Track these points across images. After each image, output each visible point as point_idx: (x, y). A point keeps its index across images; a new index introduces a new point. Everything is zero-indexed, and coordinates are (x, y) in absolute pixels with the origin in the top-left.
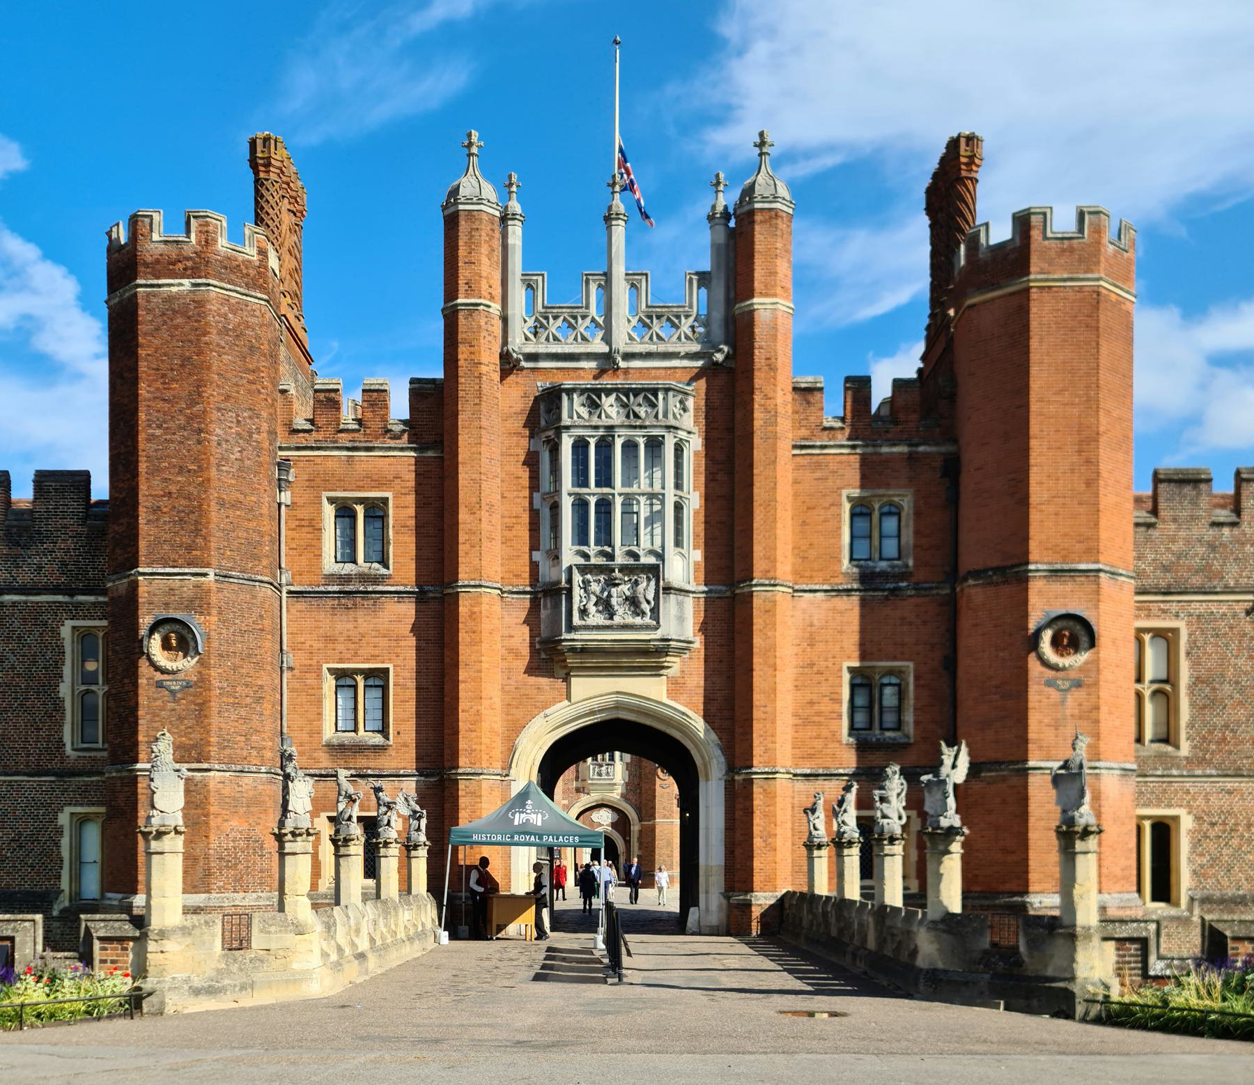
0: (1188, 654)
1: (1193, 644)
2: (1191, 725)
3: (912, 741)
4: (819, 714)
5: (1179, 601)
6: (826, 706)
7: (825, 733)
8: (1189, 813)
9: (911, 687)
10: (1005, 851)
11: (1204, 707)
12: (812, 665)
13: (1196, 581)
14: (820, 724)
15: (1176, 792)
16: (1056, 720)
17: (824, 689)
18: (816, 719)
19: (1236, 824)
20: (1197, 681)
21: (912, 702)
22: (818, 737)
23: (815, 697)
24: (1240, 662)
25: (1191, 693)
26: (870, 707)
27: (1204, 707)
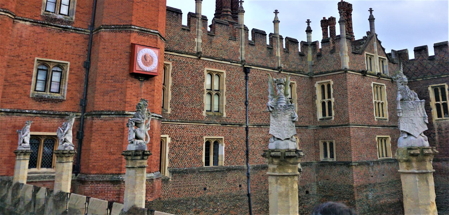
0: (172, 74)
1: (174, 70)
2: (171, 102)
3: (65, 99)
4: (19, 81)
5: (170, 54)
6: (23, 78)
7: (21, 91)
8: (169, 137)
9: (68, 73)
10: (110, 153)
11: (176, 95)
12: (18, 56)
13: (176, 48)
14: (18, 86)
15: (165, 128)
16: (138, 94)
17: (24, 69)
18: (17, 83)
19: (185, 141)
20: (174, 85)
21: (67, 80)
22: (16, 93)
23: (18, 72)
24: (188, 80)
25: (172, 90)
26: (46, 81)
27: (176, 95)
